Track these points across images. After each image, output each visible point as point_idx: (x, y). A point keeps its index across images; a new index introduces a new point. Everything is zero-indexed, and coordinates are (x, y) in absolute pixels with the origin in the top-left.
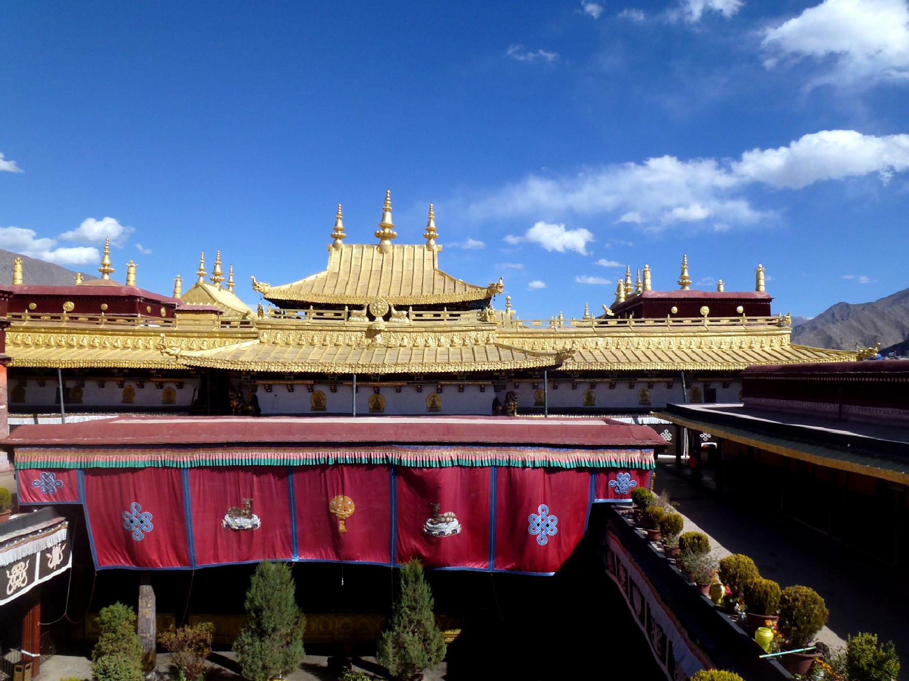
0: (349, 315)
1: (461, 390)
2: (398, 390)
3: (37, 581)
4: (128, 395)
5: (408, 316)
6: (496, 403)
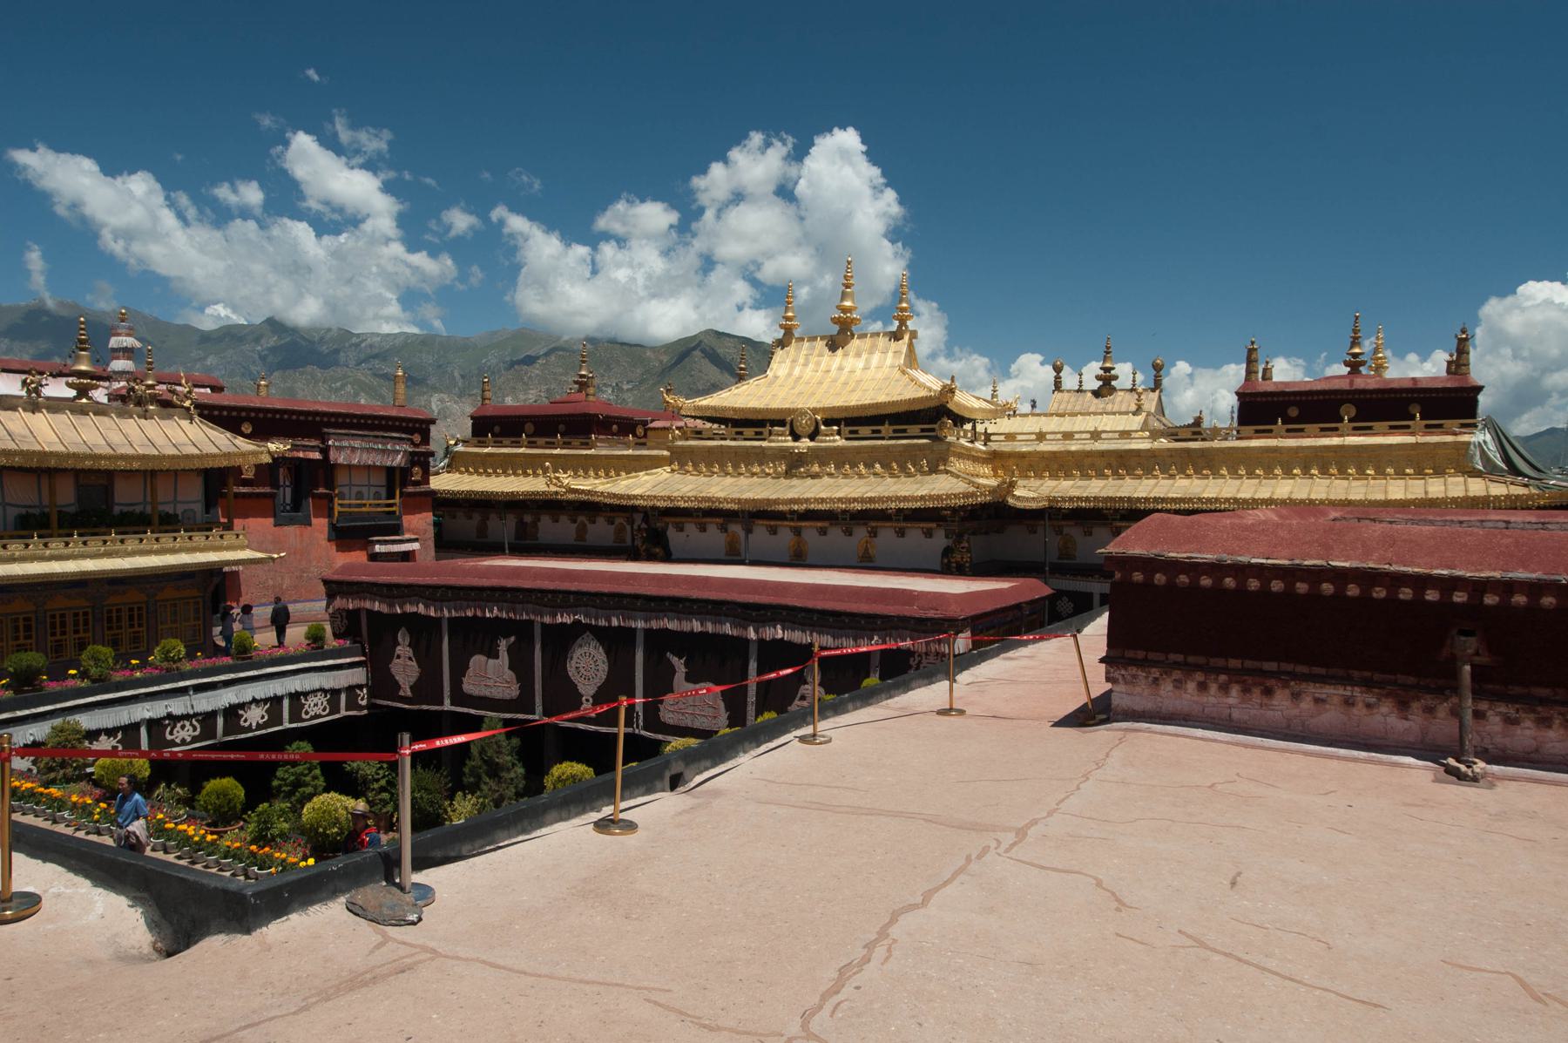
0: (770, 433)
1: (901, 533)
2: (823, 532)
3: (343, 713)
4: (582, 531)
5: (839, 433)
6: (947, 552)
